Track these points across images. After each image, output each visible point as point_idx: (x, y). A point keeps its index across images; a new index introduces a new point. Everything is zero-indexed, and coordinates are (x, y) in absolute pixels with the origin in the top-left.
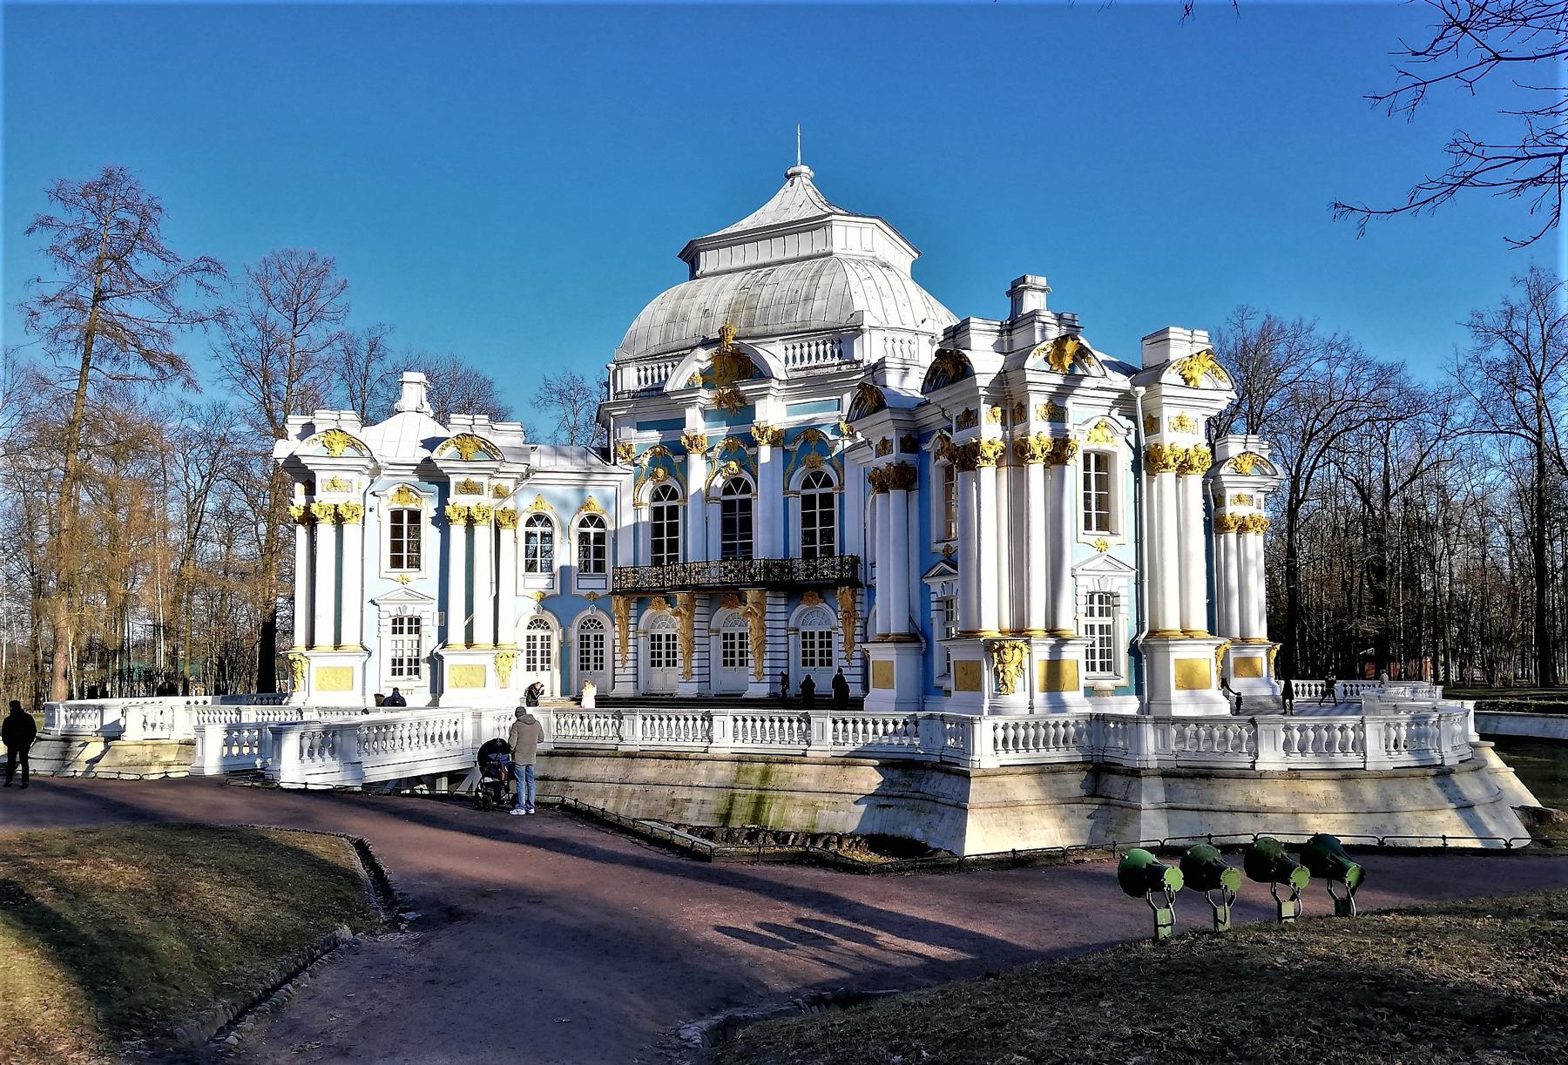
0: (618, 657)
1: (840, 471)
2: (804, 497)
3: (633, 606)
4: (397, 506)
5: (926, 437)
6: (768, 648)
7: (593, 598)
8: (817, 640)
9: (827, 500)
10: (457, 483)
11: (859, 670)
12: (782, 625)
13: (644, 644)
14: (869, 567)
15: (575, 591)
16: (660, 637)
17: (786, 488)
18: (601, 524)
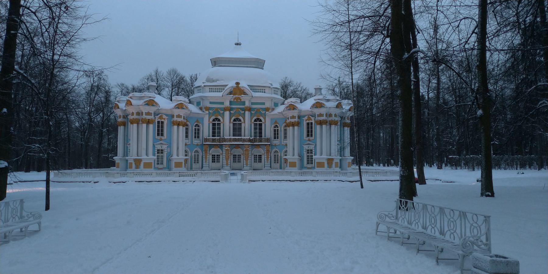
0: (204, 160)
1: (265, 119)
2: (254, 124)
3: (209, 147)
4: (159, 120)
5: (304, 116)
6: (249, 158)
7: (197, 145)
8: (258, 157)
9: (260, 125)
10: (176, 115)
11: (270, 164)
12: (251, 153)
13: (211, 157)
14: (272, 141)
15: (194, 143)
16: (215, 155)
17: (251, 122)
18: (199, 126)
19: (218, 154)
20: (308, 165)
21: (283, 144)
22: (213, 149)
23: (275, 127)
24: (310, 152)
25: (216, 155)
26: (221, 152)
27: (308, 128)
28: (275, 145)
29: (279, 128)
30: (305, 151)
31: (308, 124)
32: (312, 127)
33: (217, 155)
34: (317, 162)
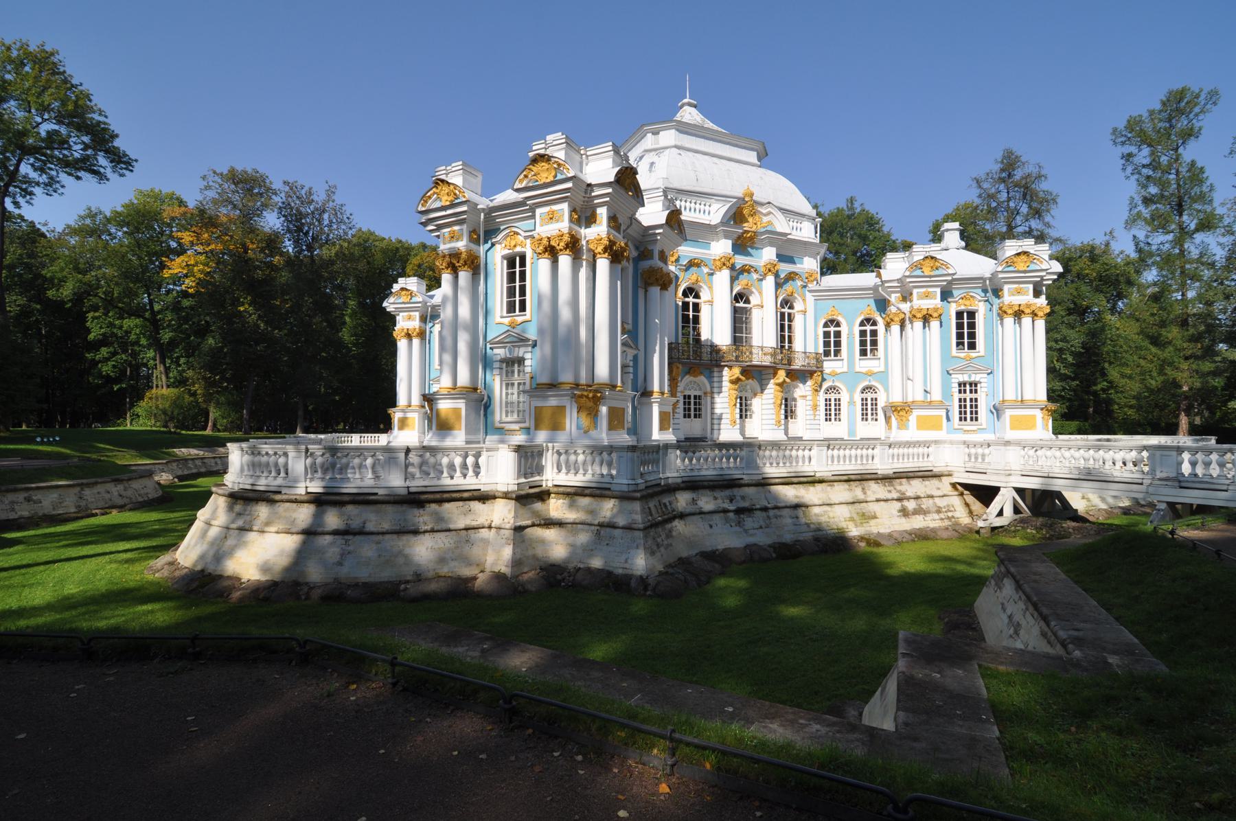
16: (689, 397)
19: (698, 393)
20: (963, 422)
21: (858, 369)
22: (687, 377)
23: (826, 325)
24: (968, 388)
25: (692, 397)
26: (709, 389)
27: (960, 326)
28: (834, 374)
29: (844, 329)
30: (957, 385)
31: (959, 315)
32: (972, 326)
33: (695, 397)
34: (1011, 416)
